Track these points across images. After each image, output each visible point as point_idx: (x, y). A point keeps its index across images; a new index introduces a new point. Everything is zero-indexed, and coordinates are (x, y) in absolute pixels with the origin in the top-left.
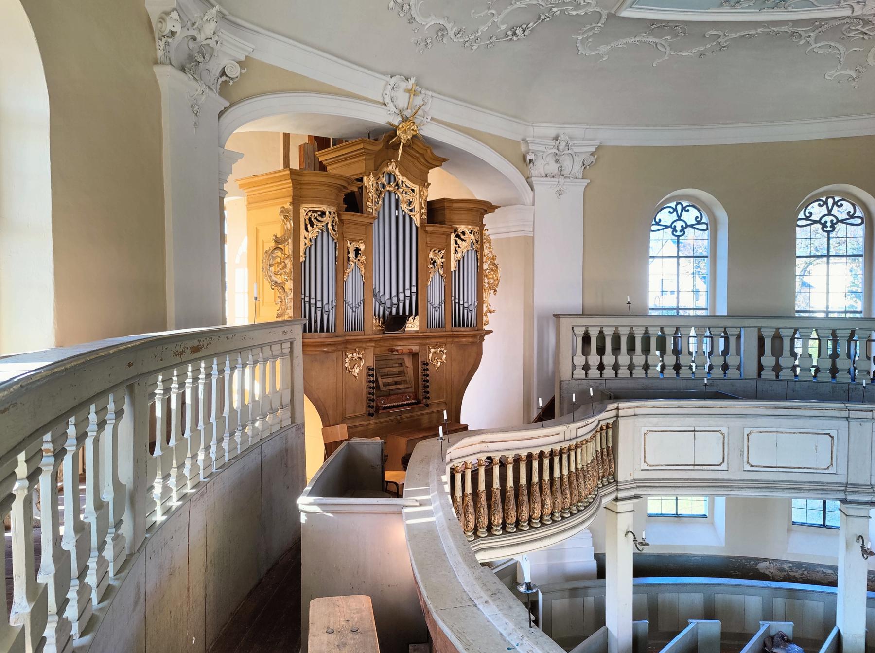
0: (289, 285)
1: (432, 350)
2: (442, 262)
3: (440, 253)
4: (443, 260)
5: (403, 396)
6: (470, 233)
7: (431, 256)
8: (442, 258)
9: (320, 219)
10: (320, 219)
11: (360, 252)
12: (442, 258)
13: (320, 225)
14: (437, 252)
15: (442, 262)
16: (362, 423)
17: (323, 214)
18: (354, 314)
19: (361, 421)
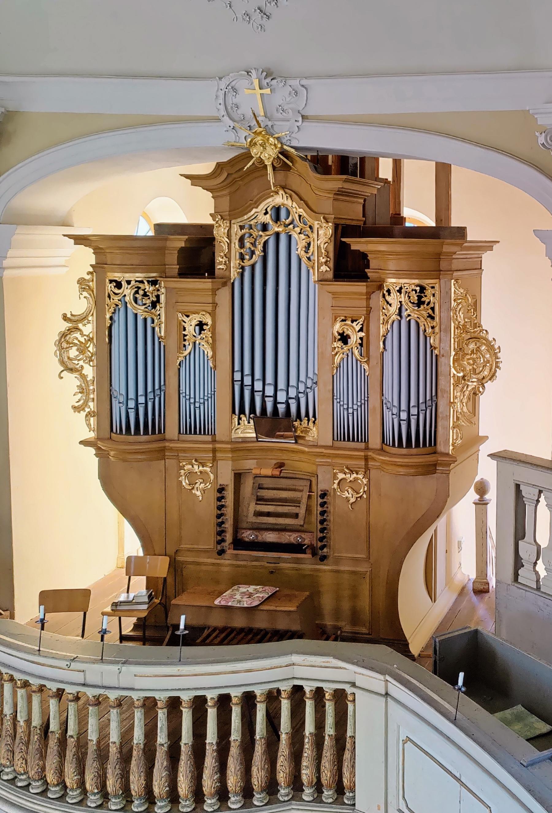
0: (89, 371)
1: (341, 476)
2: (361, 339)
3: (355, 323)
4: (362, 334)
5: (290, 536)
6: (398, 291)
7: (338, 327)
8: (361, 330)
9: (117, 291)
10: (117, 291)
11: (205, 327)
12: (361, 330)
13: (116, 298)
14: (349, 322)
15: (361, 339)
16: (209, 561)
17: (119, 285)
18: (197, 411)
19: (208, 558)
